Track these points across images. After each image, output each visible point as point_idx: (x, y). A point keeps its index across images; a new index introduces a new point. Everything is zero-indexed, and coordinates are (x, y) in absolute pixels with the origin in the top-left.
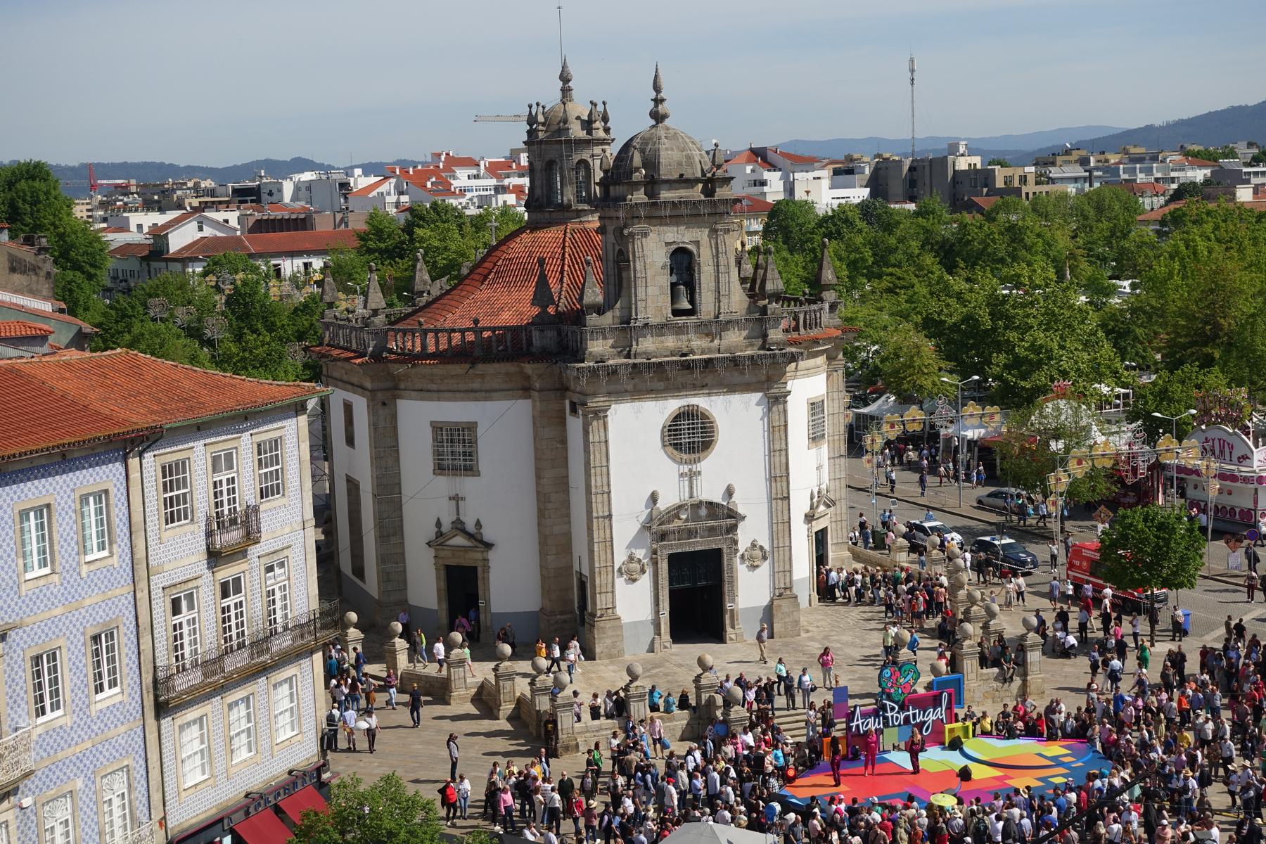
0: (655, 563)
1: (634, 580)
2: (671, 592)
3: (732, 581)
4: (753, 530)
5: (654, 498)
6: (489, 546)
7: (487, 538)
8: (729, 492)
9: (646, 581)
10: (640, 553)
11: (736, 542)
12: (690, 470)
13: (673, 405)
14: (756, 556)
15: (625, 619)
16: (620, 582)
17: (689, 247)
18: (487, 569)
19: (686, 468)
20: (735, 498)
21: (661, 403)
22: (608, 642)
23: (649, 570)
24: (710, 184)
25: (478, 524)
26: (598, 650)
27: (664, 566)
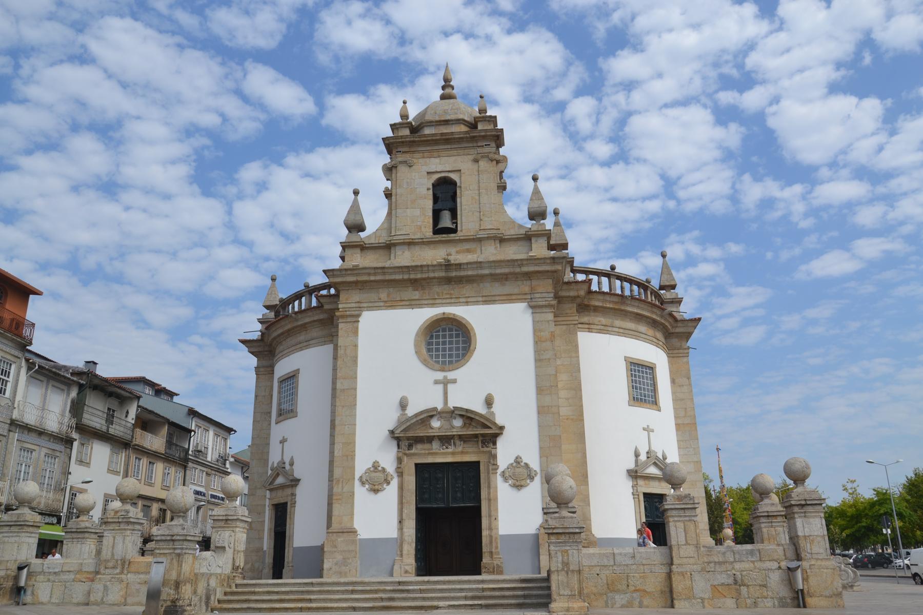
0: (400, 474)
1: (376, 491)
2: (418, 510)
3: (493, 500)
4: (518, 443)
5: (403, 405)
6: (295, 482)
7: (297, 475)
8: (489, 402)
9: (392, 491)
10: (388, 459)
11: (495, 457)
12: (445, 377)
13: (427, 314)
14: (519, 476)
15: (364, 532)
16: (361, 493)
17: (453, 176)
18: (294, 504)
19: (440, 375)
20: (496, 408)
21: (417, 311)
22: (339, 557)
23: (395, 483)
24: (473, 126)
25: (292, 464)
26: (326, 566)
27: (411, 480)
